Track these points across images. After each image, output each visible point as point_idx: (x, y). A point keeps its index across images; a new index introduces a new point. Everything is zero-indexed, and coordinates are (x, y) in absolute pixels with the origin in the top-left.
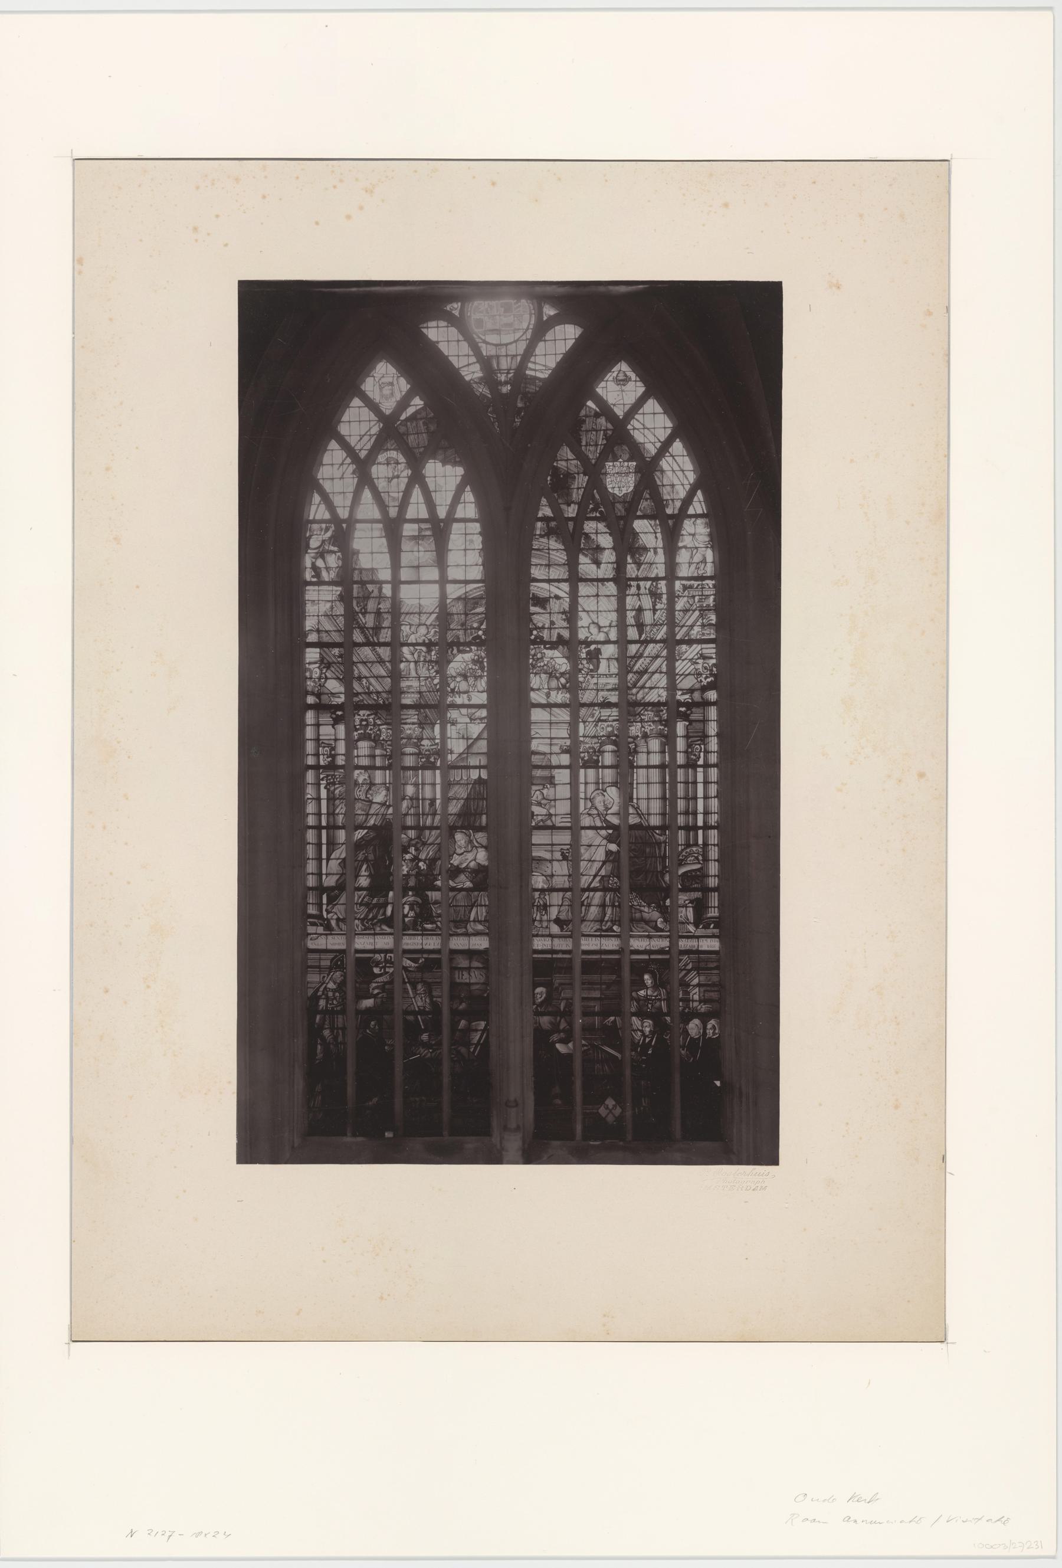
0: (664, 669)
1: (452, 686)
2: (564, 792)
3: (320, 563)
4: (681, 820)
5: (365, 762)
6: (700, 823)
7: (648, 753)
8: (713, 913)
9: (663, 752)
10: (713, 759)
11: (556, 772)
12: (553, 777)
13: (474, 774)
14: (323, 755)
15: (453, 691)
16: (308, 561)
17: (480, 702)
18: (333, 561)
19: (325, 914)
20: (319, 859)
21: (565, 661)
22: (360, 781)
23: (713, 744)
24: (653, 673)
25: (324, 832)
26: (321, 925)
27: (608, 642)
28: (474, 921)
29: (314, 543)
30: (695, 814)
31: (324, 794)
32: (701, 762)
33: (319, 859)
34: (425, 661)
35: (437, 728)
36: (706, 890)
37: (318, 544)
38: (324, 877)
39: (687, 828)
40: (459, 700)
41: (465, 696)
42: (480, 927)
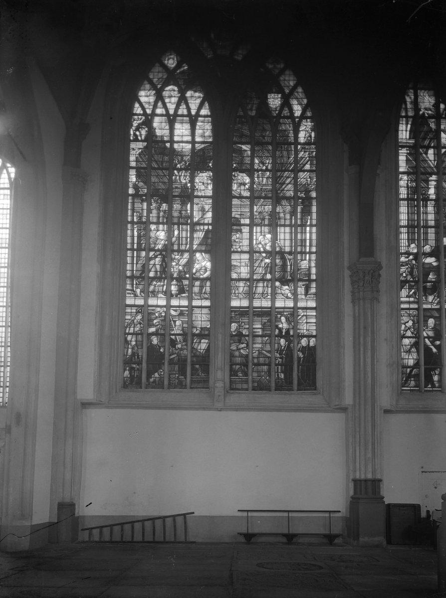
0: (293, 182)
1: (197, 187)
2: (246, 235)
3: (138, 133)
4: (299, 249)
5: (155, 220)
6: (308, 250)
7: (285, 219)
8: (313, 290)
9: (291, 219)
10: (314, 222)
11: (242, 227)
12: (241, 230)
13: (206, 227)
14: (136, 216)
15: (197, 189)
16: (132, 132)
17: (210, 195)
18: (144, 132)
19: (134, 289)
20: (132, 263)
21: (248, 178)
22: (152, 229)
23: (314, 216)
24: (288, 184)
25: (135, 252)
26: (133, 294)
27: (267, 170)
28: (204, 293)
29: (135, 124)
30: (305, 246)
31: (136, 233)
32: (309, 223)
33: (132, 263)
34: (184, 176)
35: (189, 206)
36: (310, 281)
37: (137, 124)
38: (135, 272)
39: (301, 253)
40: (200, 194)
41: (203, 192)
42: (206, 296)
